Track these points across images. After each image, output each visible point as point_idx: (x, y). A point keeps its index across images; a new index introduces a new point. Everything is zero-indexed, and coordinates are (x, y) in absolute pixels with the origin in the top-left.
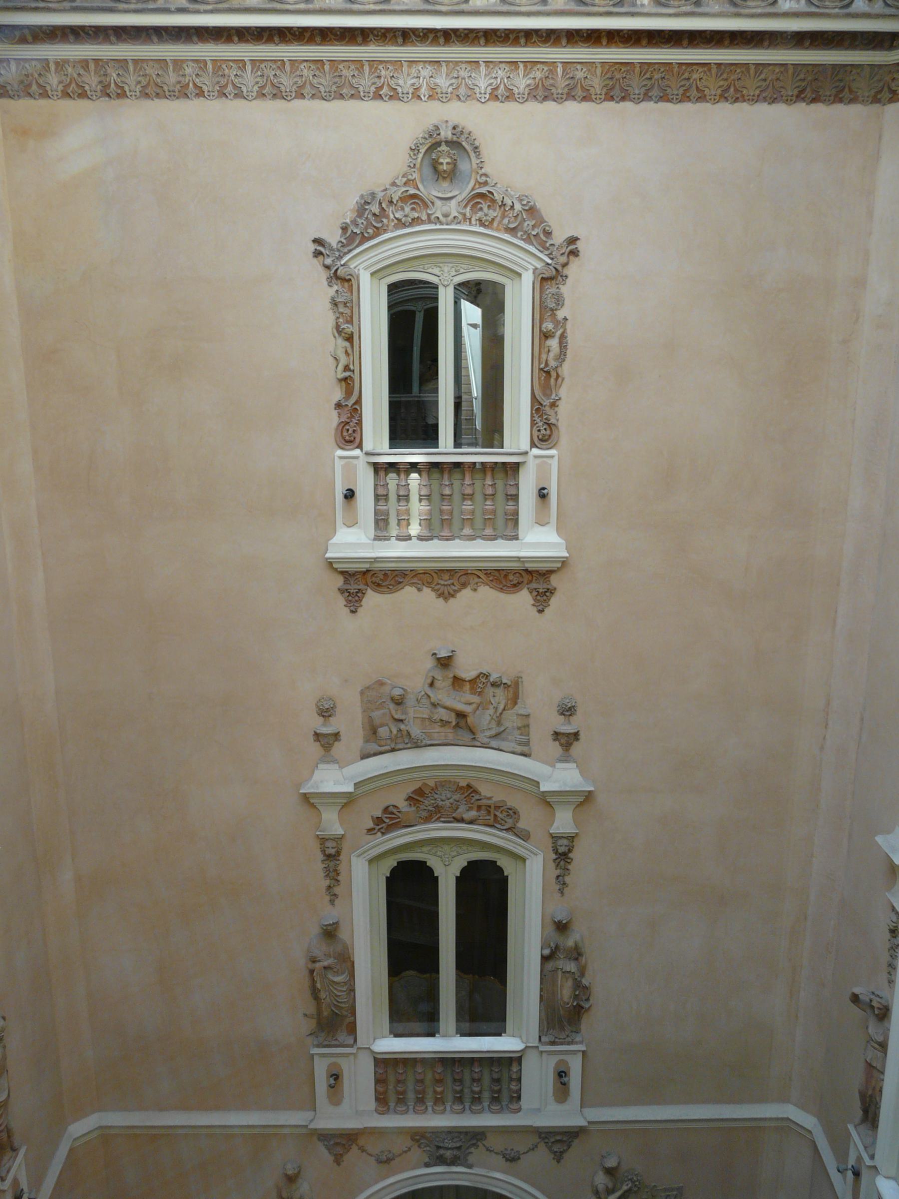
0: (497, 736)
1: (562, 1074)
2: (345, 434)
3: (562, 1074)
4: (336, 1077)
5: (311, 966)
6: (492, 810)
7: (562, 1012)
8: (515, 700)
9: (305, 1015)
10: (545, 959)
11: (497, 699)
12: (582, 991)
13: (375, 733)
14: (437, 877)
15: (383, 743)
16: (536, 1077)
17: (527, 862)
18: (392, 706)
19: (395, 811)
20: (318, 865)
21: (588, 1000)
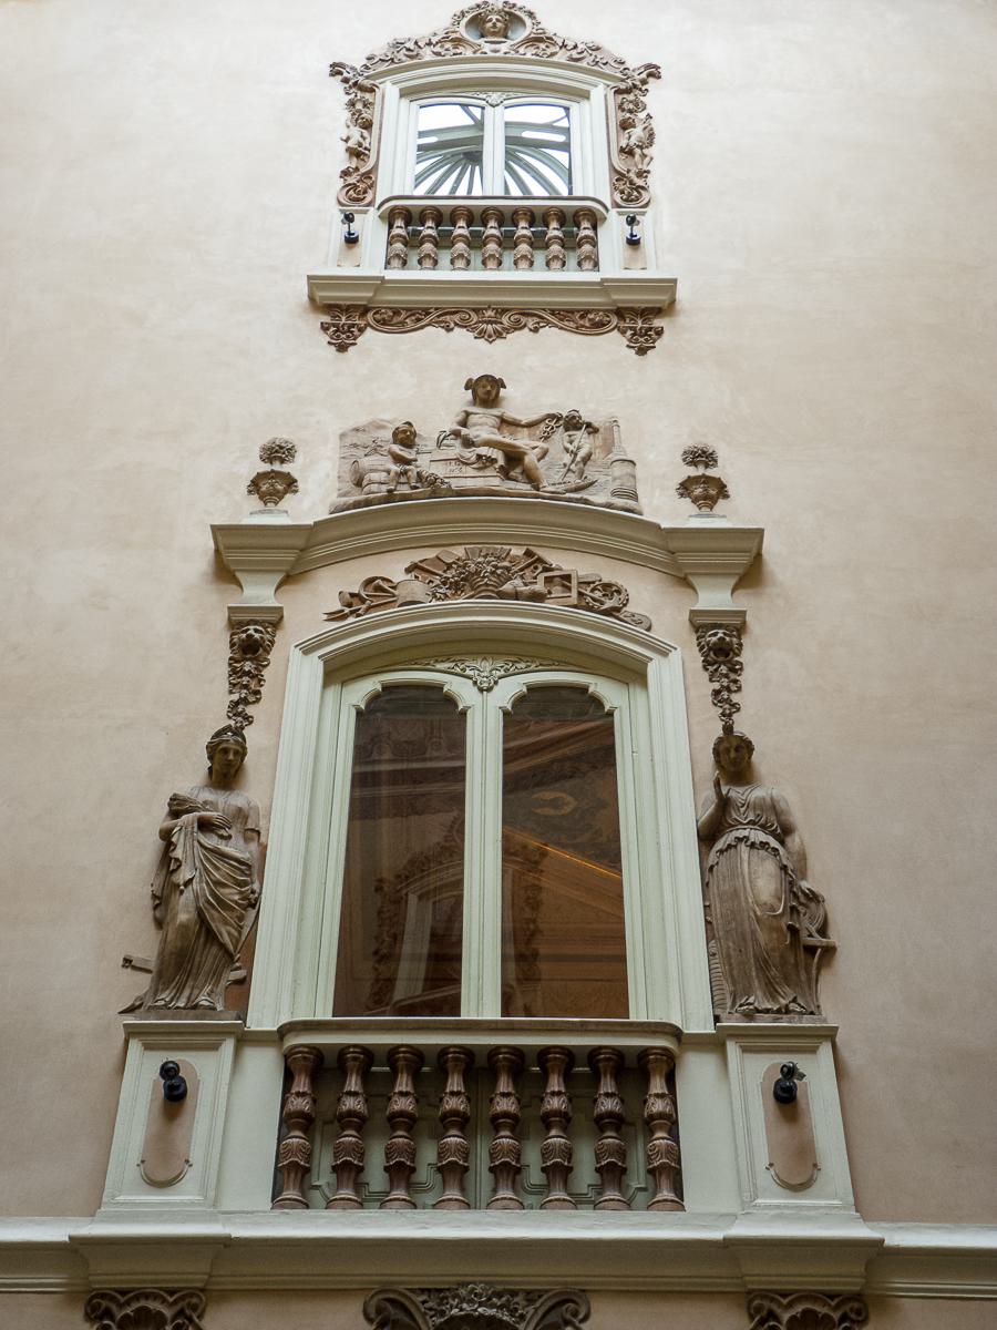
0: (578, 489)
1: (786, 1095)
2: (351, 192)
3: (786, 1095)
4: (174, 1092)
5: (169, 823)
6: (574, 583)
7: (762, 937)
8: (608, 447)
9: (128, 962)
10: (709, 835)
11: (576, 443)
12: (800, 900)
13: (359, 483)
14: (464, 714)
15: (374, 487)
16: (718, 1107)
17: (651, 669)
18: (397, 448)
19: (386, 586)
20: (218, 651)
21: (823, 931)
